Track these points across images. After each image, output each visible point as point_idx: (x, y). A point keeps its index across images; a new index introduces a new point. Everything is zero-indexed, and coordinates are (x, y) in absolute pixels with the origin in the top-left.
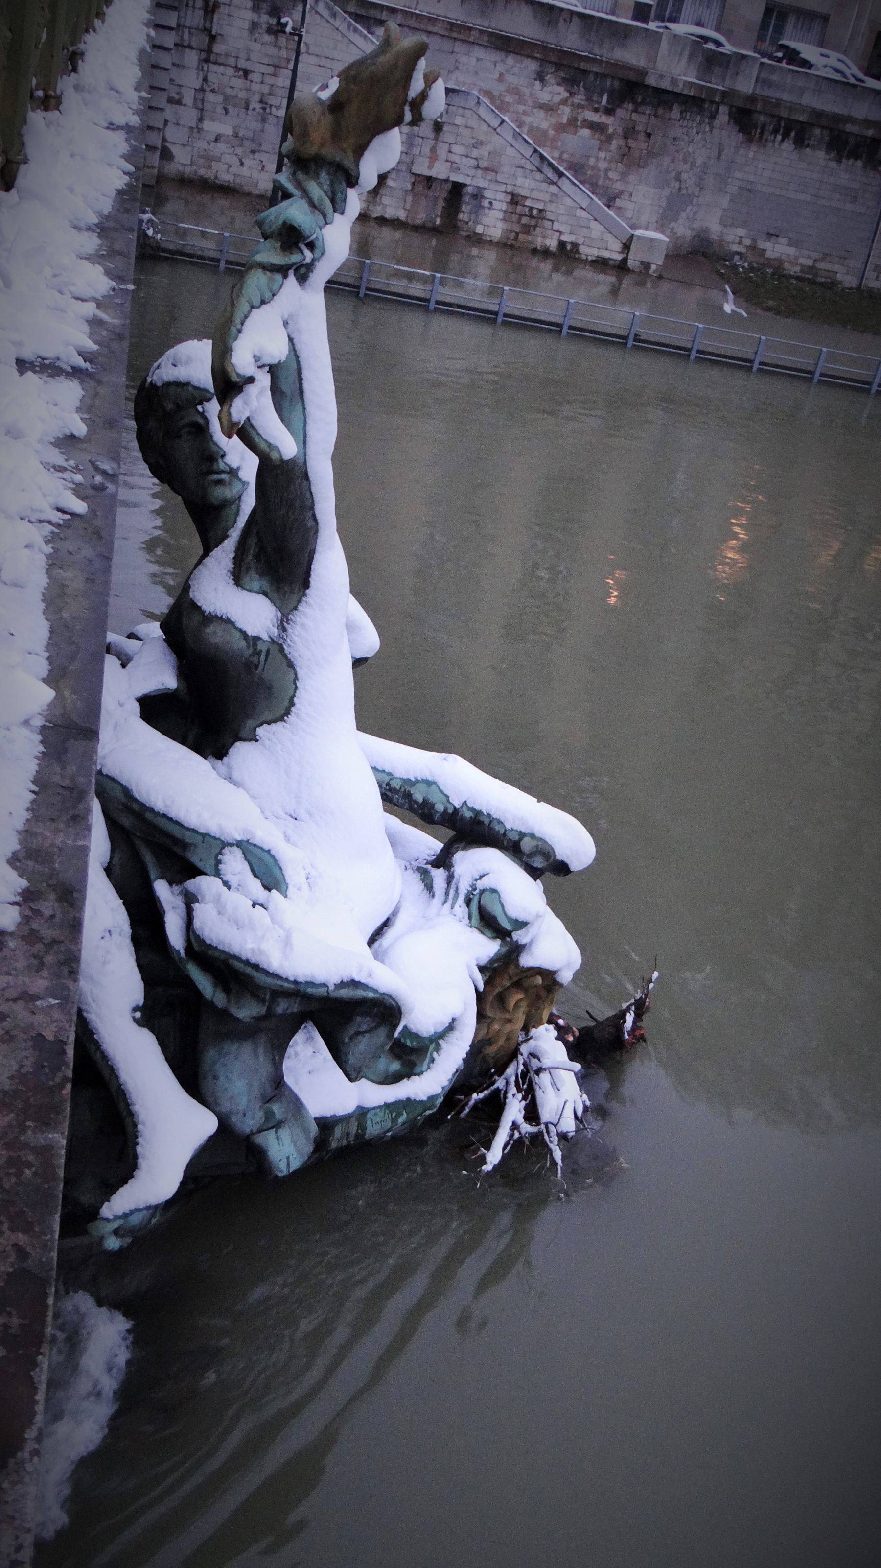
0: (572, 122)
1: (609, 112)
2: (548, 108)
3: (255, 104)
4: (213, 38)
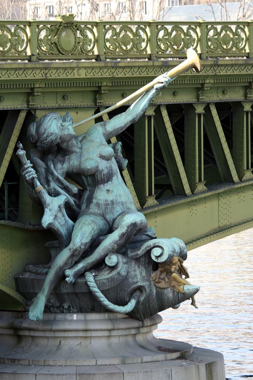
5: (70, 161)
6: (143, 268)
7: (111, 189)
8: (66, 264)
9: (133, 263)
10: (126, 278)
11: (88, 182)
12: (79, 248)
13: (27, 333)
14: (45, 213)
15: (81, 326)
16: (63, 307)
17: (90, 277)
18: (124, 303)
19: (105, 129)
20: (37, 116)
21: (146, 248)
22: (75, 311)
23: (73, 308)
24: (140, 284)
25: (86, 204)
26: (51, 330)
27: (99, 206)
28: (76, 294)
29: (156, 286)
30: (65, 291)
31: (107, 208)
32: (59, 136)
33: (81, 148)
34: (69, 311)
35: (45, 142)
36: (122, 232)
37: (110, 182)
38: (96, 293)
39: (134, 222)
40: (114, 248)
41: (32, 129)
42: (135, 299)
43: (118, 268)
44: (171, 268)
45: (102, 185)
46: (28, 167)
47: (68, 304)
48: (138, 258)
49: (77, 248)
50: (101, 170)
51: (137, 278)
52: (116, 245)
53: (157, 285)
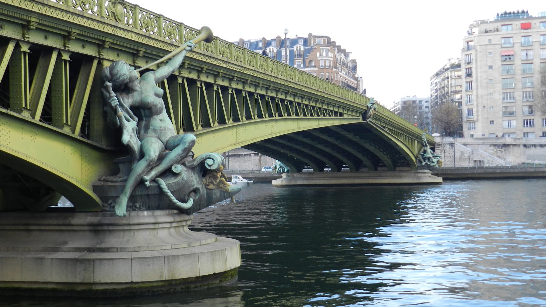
0: (497, 151)
1: (501, 148)
2: (493, 150)
3: (451, 157)
4: (445, 150)
5: (133, 97)
6: (197, 175)
7: (163, 119)
8: (143, 172)
9: (190, 171)
10: (186, 182)
11: (145, 114)
12: (154, 160)
13: (106, 228)
14: (124, 133)
15: (152, 220)
16: (135, 207)
17: (162, 182)
18: (185, 202)
19: (155, 76)
20: (104, 64)
21: (200, 160)
22: (144, 209)
23: (143, 207)
24: (196, 186)
25: (144, 130)
26: (129, 225)
27: (155, 131)
28: (148, 195)
29: (207, 188)
30: (140, 194)
31: (162, 133)
32: (129, 77)
33: (141, 88)
34: (140, 209)
35: (118, 80)
36: (185, 147)
37: (161, 114)
38: (168, 194)
39: (193, 140)
40: (178, 160)
41: (106, 71)
42: (192, 198)
43: (182, 174)
44: (217, 174)
45: (156, 116)
46: (113, 96)
47: (140, 204)
48: (194, 167)
49: (152, 159)
50: (156, 104)
51: (194, 182)
52: (180, 157)
53: (207, 187)
